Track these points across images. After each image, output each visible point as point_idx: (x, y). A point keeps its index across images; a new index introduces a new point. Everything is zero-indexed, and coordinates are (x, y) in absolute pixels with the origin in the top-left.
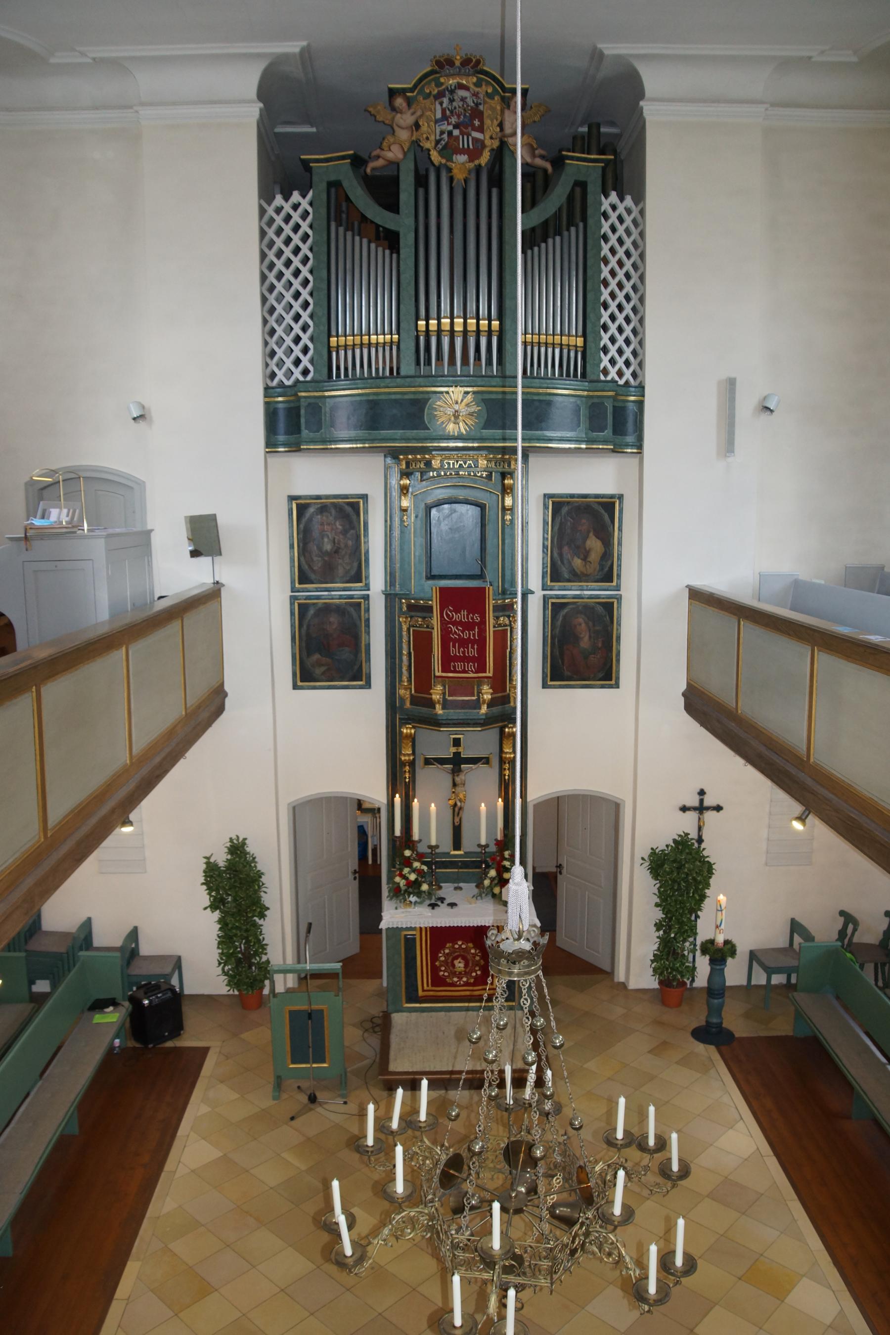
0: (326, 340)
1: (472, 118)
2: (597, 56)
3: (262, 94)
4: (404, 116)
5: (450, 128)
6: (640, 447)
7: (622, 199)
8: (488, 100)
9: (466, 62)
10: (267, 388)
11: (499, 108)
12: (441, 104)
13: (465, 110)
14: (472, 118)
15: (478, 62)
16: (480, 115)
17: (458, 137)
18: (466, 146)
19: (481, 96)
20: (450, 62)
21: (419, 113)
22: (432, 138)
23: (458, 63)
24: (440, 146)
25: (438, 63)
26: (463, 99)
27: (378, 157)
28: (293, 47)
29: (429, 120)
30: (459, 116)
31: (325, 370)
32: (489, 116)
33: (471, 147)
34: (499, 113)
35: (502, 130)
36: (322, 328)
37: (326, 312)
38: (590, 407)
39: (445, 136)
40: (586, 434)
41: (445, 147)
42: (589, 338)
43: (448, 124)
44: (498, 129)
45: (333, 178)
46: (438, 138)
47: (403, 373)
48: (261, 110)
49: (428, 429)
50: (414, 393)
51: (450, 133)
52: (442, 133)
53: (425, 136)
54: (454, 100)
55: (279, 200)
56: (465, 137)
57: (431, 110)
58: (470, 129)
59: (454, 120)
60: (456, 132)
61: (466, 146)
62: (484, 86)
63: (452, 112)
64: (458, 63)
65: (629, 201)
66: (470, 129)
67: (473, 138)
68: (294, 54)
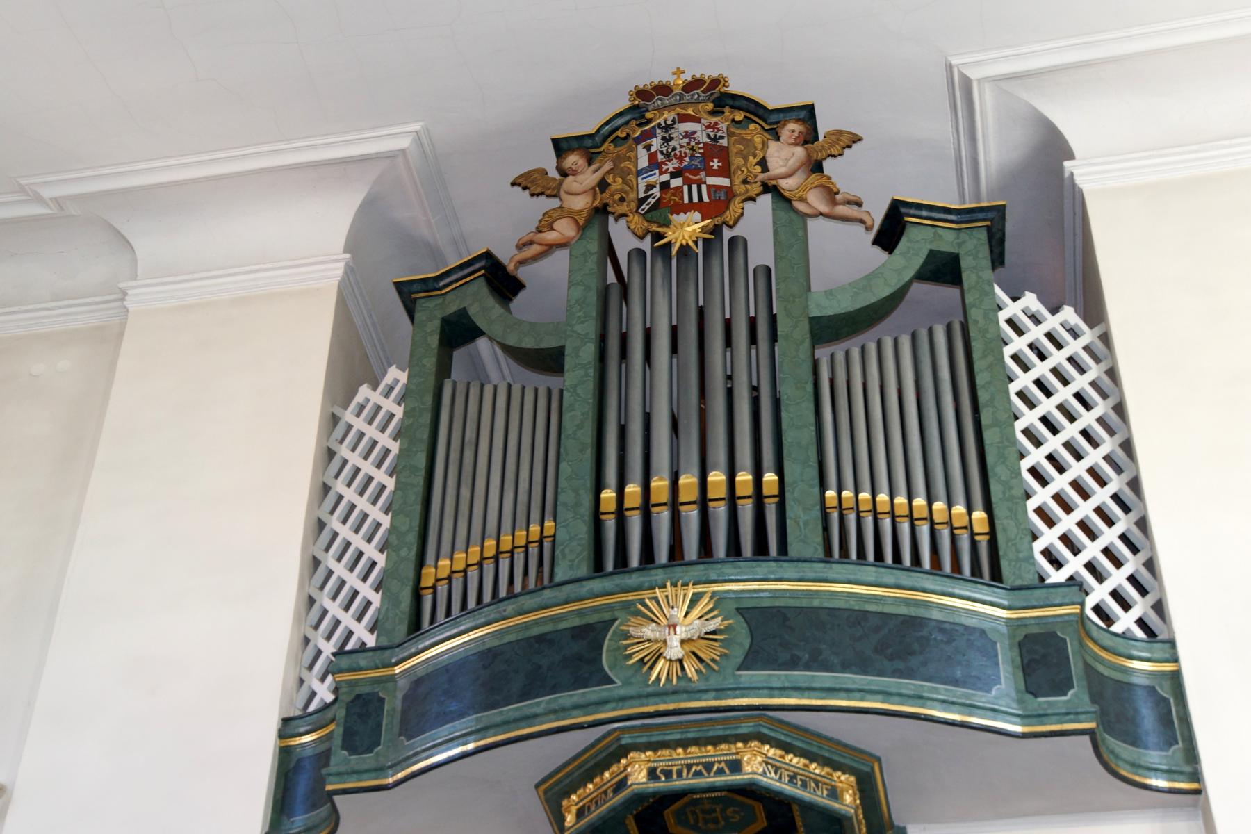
0: (411, 574)
1: (707, 158)
2: (961, 93)
3: (352, 245)
4: (580, 178)
5: (666, 177)
6: (1196, 776)
7: (1054, 311)
8: (733, 130)
9: (694, 84)
10: (286, 721)
11: (757, 140)
12: (648, 147)
13: (692, 149)
14: (707, 158)
15: (715, 82)
16: (724, 154)
17: (679, 190)
18: (695, 199)
19: (723, 127)
20: (664, 89)
21: (608, 166)
22: (632, 196)
23: (677, 91)
24: (645, 207)
25: (642, 94)
26: (687, 135)
27: (531, 243)
28: (396, 138)
29: (624, 174)
30: (681, 159)
31: (402, 629)
32: (739, 153)
33: (706, 199)
34: (760, 147)
35: (765, 169)
36: (404, 552)
37: (416, 522)
38: (1020, 645)
39: (656, 191)
40: (1020, 702)
41: (654, 207)
42: (999, 511)
43: (661, 173)
44: (759, 169)
45: (452, 308)
46: (641, 195)
47: (559, 577)
48: (347, 265)
49: (612, 682)
50: (579, 613)
51: (665, 186)
52: (650, 187)
53: (617, 197)
54: (671, 139)
55: (364, 392)
56: (694, 187)
57: (629, 159)
58: (703, 174)
59: (671, 166)
60: (676, 182)
61: (695, 199)
62: (727, 114)
63: (667, 156)
64: (677, 91)
65: (1069, 314)
66: (703, 174)
67: (709, 187)
68: (403, 151)
